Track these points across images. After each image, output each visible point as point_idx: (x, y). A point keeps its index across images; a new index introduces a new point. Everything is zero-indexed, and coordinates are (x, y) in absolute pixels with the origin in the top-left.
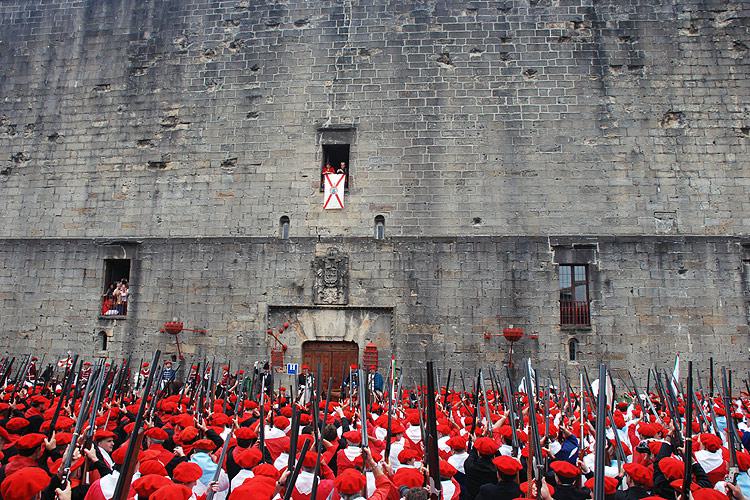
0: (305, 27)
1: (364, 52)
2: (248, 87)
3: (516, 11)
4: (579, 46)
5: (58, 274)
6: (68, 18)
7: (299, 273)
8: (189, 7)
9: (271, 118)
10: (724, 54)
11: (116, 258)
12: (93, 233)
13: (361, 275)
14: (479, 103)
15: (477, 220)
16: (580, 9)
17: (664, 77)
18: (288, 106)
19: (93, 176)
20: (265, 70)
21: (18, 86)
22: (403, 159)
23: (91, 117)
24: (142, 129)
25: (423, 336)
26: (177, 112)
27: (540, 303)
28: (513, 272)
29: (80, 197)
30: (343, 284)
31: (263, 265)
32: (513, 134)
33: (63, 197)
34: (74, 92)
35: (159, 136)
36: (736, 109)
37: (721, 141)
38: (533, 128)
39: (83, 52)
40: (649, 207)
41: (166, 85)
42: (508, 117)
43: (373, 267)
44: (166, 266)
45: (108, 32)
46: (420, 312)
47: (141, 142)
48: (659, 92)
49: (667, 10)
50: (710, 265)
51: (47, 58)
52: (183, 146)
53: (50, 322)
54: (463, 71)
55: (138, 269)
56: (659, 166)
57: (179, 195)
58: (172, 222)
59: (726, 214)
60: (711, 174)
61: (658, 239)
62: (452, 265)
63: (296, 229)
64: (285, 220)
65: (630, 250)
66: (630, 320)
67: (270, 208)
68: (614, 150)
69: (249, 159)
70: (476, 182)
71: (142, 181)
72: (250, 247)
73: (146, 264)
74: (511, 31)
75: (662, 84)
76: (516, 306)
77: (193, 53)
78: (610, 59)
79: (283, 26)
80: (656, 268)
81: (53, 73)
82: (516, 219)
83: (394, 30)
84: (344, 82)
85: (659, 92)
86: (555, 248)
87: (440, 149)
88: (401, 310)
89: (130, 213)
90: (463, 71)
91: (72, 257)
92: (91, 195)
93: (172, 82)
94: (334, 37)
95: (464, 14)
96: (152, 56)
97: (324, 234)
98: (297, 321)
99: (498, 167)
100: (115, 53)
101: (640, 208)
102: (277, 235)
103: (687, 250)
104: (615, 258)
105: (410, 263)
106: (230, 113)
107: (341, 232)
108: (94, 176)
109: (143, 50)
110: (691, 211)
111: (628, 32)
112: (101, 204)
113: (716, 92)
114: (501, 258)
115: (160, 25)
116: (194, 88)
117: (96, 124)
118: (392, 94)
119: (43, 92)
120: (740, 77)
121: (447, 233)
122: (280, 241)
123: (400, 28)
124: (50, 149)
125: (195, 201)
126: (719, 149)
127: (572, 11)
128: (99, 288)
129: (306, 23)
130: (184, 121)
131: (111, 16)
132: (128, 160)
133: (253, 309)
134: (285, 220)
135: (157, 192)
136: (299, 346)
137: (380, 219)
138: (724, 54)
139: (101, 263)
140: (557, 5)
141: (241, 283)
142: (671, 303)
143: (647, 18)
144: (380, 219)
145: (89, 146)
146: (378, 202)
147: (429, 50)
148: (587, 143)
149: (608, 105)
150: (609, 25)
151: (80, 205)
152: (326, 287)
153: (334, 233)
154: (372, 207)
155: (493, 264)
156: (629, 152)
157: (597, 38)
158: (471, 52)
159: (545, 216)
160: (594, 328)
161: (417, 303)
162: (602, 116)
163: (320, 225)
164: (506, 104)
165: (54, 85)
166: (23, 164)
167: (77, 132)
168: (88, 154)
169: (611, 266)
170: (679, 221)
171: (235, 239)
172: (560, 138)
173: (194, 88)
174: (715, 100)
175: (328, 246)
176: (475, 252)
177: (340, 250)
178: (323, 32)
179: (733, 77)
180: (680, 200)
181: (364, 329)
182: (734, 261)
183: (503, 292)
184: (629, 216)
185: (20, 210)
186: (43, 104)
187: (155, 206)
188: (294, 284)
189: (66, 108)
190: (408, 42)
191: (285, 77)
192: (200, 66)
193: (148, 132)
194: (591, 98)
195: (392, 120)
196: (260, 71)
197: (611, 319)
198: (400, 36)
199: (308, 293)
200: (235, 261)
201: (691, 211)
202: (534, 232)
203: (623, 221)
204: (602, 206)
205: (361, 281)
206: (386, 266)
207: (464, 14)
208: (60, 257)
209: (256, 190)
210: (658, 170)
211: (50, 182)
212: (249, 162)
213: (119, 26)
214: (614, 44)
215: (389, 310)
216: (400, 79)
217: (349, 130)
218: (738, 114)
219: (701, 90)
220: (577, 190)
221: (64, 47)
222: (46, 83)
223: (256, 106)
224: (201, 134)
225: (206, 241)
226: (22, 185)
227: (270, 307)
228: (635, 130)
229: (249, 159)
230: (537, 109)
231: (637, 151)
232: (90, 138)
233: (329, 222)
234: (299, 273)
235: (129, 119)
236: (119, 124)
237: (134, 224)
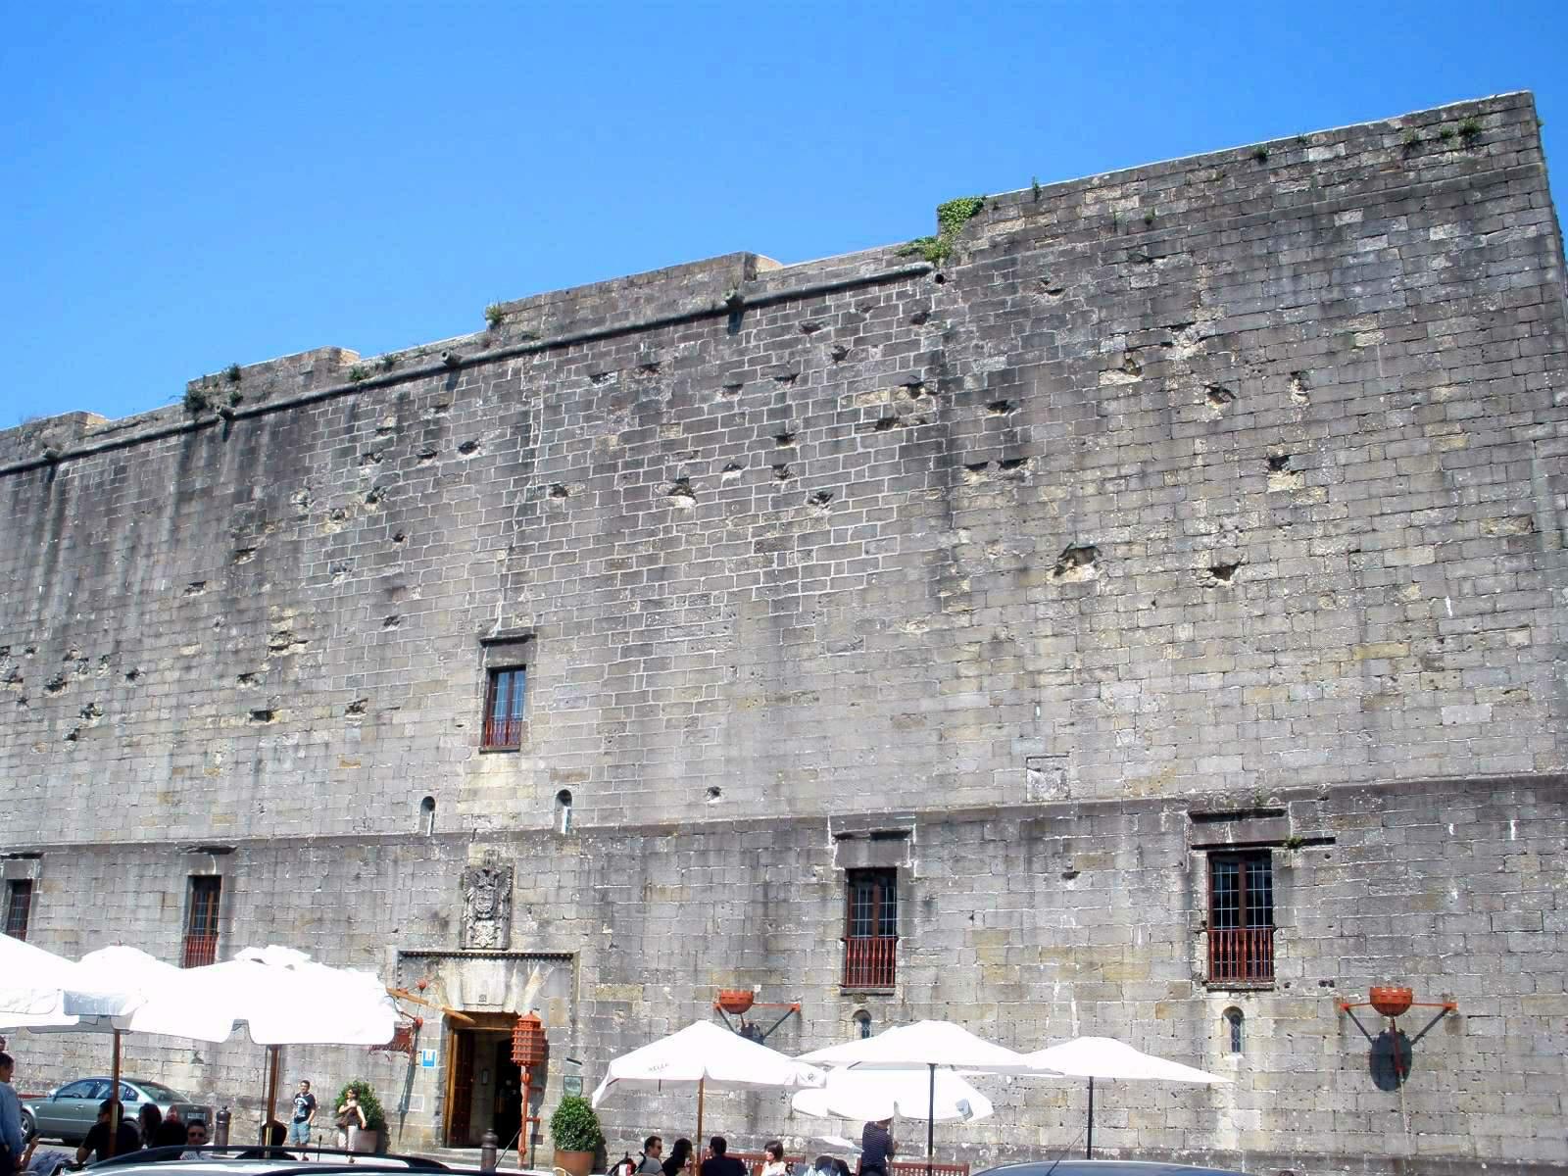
0: (473, 455)
1: (559, 491)
2: (389, 572)
3: (805, 381)
4: (910, 432)
5: (130, 901)
6: (158, 473)
7: (443, 896)
8: (314, 437)
9: (416, 626)
10: (1185, 415)
11: (203, 873)
12: (180, 833)
13: (532, 896)
14: (731, 570)
15: (716, 792)
16: (918, 359)
17: (1064, 477)
18: (443, 603)
19: (179, 738)
20: (414, 540)
21: (94, 593)
22: (605, 684)
23: (181, 639)
24: (244, 655)
25: (618, 1005)
26: (290, 622)
27: (808, 945)
28: (766, 885)
30: (501, 911)
31: (394, 885)
32: (783, 625)
33: (143, 775)
34: (162, 598)
35: (266, 667)
36: (1202, 527)
37: (1167, 599)
38: (818, 608)
39: (175, 529)
40: (1018, 747)
41: (278, 577)
42: (776, 590)
43: (548, 883)
44: (266, 886)
45: (206, 492)
46: (614, 962)
47: (244, 678)
48: (1054, 509)
49: (1079, 338)
50: (1125, 859)
51: (128, 544)
52: (297, 683)
54: (708, 511)
55: (231, 893)
56: (1041, 664)
58: (279, 813)
59: (1167, 752)
60: (1141, 670)
61: (1028, 811)
62: (667, 877)
63: (443, 820)
64: (429, 803)
65: (972, 836)
67: (409, 784)
68: (960, 638)
69: (383, 702)
70: (716, 722)
71: (242, 744)
72: (379, 851)
73: (241, 884)
74: (796, 421)
75: (1060, 493)
76: (767, 948)
77: (317, 518)
78: (967, 454)
79: (442, 456)
80: (1020, 870)
81: (136, 568)
82: (777, 786)
83: (605, 442)
84: (525, 550)
85: (1054, 509)
86: (839, 838)
87: (662, 664)
88: (585, 963)
89: (224, 798)
90: (708, 511)
91: (149, 872)
92: (175, 770)
93: (286, 571)
94: (512, 469)
95: (719, 398)
96: (261, 528)
97: (483, 826)
98: (438, 978)
99: (754, 689)
100: (214, 524)
101: (1002, 750)
102: (416, 829)
103: (1081, 833)
104: (945, 853)
105: (603, 874)
106: (359, 622)
107: (506, 822)
108: (180, 740)
109: (250, 517)
110: (1097, 750)
111: (1003, 393)
112: (188, 783)
113: (1162, 496)
114: (747, 862)
115: (276, 474)
116: (314, 579)
117: (188, 651)
118: (593, 567)
119: (122, 602)
120: (1211, 459)
121: (666, 817)
122: (419, 840)
123: (614, 439)
124: (129, 695)
125: (308, 777)
126: (1164, 616)
127: (904, 364)
128: (181, 923)
129: (475, 447)
130: (299, 637)
131: (212, 462)
132: (227, 709)
133: (379, 956)
134: (429, 803)
135: (260, 761)
136: (439, 1019)
137: (565, 797)
138: (1185, 415)
139: (185, 880)
140: (878, 357)
141: (364, 914)
142: (1044, 941)
143: (1041, 358)
144: (565, 797)
145: (175, 688)
146: (563, 767)
147: (655, 476)
148: (911, 628)
149: (955, 547)
150: (969, 384)
151: (161, 787)
152: (479, 919)
153: (497, 824)
154: (555, 775)
155: (733, 873)
156: (987, 638)
157: (944, 414)
158: (727, 469)
159: (827, 777)
160: (899, 991)
161: (611, 946)
162: (942, 571)
163: (476, 812)
164: (775, 566)
165: (136, 589)
166: (95, 721)
167: (162, 665)
168: (173, 701)
169: (936, 870)
170: (1072, 773)
171: (360, 839)
172: (864, 624)
173: (314, 579)
174: (1161, 513)
175: (486, 846)
176: (703, 853)
177: (504, 855)
178: (499, 462)
179: (1199, 461)
180: (1077, 729)
181: (533, 988)
182: (1173, 848)
183: (748, 925)
184: (981, 769)
185: (88, 798)
186: (121, 621)
187: (256, 785)
188: (435, 915)
189: (149, 625)
190: (626, 465)
191: (440, 549)
192: (323, 541)
193: (252, 661)
194: (928, 539)
195: (590, 616)
196: (407, 541)
197: (932, 971)
198: (616, 455)
199: (454, 928)
200: (358, 877)
201: (1097, 750)
202: (805, 809)
203: (967, 779)
204: (931, 752)
205: (529, 908)
206: (569, 881)
207: (719, 398)
208: (134, 872)
209: (391, 753)
210: (1040, 672)
211: (126, 750)
212: (383, 705)
213: (222, 480)
214: (977, 421)
215: (568, 958)
216: (612, 534)
217: (523, 639)
218: (1206, 540)
219: (1135, 496)
220: (887, 723)
221: (152, 522)
222: (126, 586)
223: (398, 607)
224: (320, 658)
225: (322, 842)
226: (92, 757)
227: (401, 953)
228: (1001, 591)
229: (383, 702)
230: (826, 570)
231: (1003, 635)
232: (176, 674)
233: (489, 805)
234: (443, 896)
235: (230, 638)
236: (216, 649)
237: (229, 817)
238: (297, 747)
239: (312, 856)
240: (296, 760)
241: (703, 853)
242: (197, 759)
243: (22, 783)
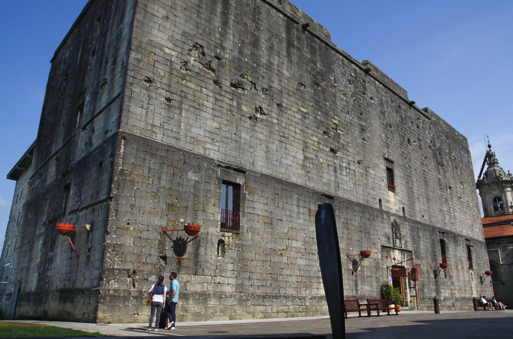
29: (300, 156)
53: (294, 244)
57: (344, 173)
66: (453, 263)
92: (306, 158)
133: (377, 246)
134: (380, 200)
215: (410, 252)
237: (328, 185)
238: (346, 168)
239: (357, 208)
240: (346, 172)
241: (425, 230)
242: (314, 157)
243: (224, 128)
